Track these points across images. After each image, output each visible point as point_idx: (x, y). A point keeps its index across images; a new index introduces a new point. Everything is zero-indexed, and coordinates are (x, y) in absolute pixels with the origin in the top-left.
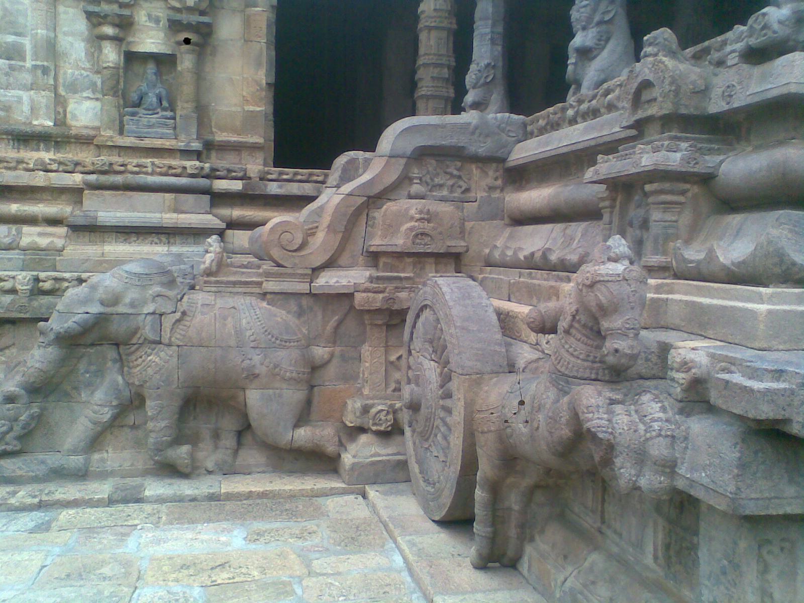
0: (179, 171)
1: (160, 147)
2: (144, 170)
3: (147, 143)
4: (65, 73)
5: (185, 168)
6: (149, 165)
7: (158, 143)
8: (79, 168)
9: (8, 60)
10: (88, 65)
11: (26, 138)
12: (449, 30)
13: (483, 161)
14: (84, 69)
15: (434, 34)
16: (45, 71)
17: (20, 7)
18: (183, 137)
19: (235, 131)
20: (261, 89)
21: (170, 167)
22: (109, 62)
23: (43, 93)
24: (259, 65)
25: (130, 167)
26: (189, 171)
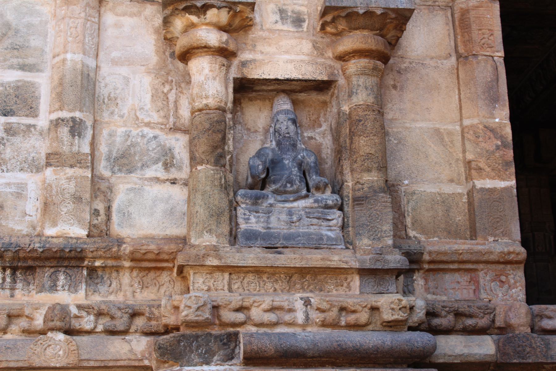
0: (363, 317)
2: (287, 317)
4: (111, 135)
5: (374, 309)
6: (299, 305)
7: (315, 259)
8: (140, 322)
9: (5, 115)
10: (156, 117)
11: (30, 263)
14: (148, 125)
16: (76, 128)
17: (36, 20)
18: (364, 242)
19: (453, 233)
20: (504, 145)
22: (207, 97)
23: (70, 172)
24: (494, 100)
25: (256, 313)
26: (387, 316)
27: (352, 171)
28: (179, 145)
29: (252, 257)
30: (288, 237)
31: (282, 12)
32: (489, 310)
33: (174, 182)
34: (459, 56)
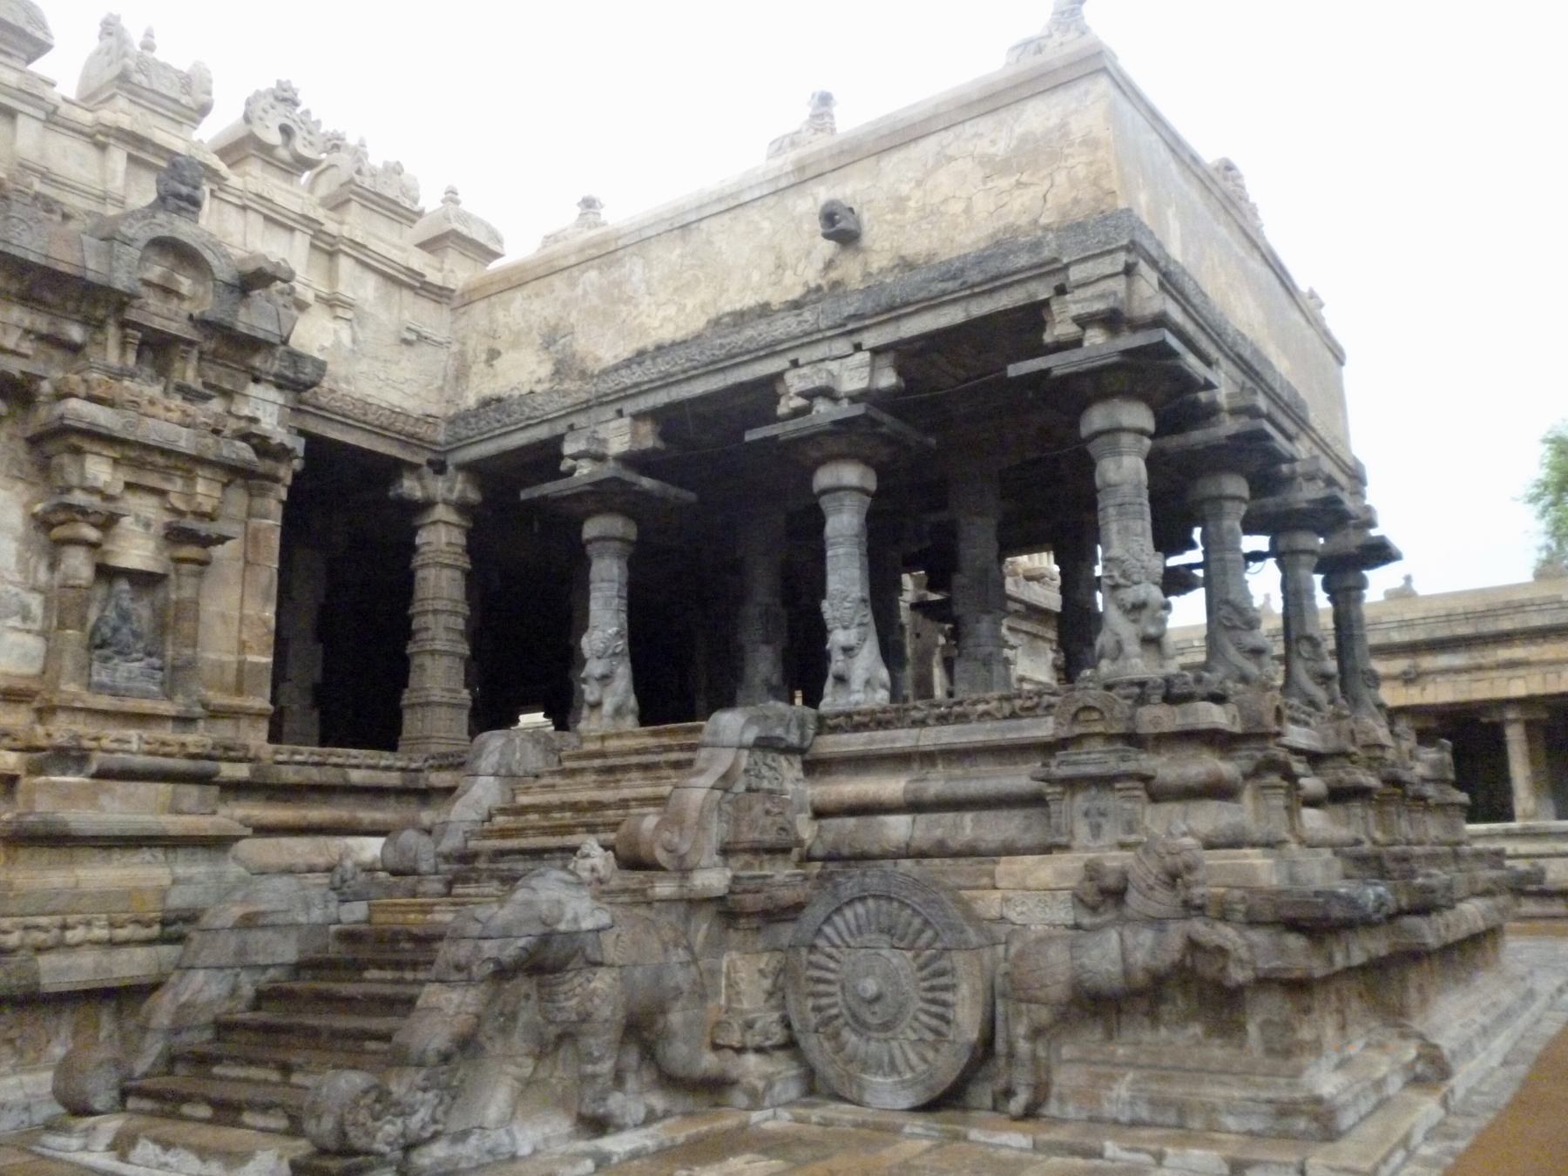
0: (175, 749)
1: (148, 711)
2: (126, 746)
3: (130, 705)
5: (183, 745)
6: (135, 739)
7: (147, 706)
10: (18, 578)
12: (464, 571)
13: (789, 750)
14: (11, 583)
15: (447, 573)
19: (223, 689)
21: (164, 744)
24: (266, 599)
25: (105, 743)
26: (193, 750)
27: (174, 644)
28: (35, 603)
29: (104, 702)
30: (127, 689)
31: (137, 517)
32: (246, 748)
33: (29, 631)
34: (247, 562)
